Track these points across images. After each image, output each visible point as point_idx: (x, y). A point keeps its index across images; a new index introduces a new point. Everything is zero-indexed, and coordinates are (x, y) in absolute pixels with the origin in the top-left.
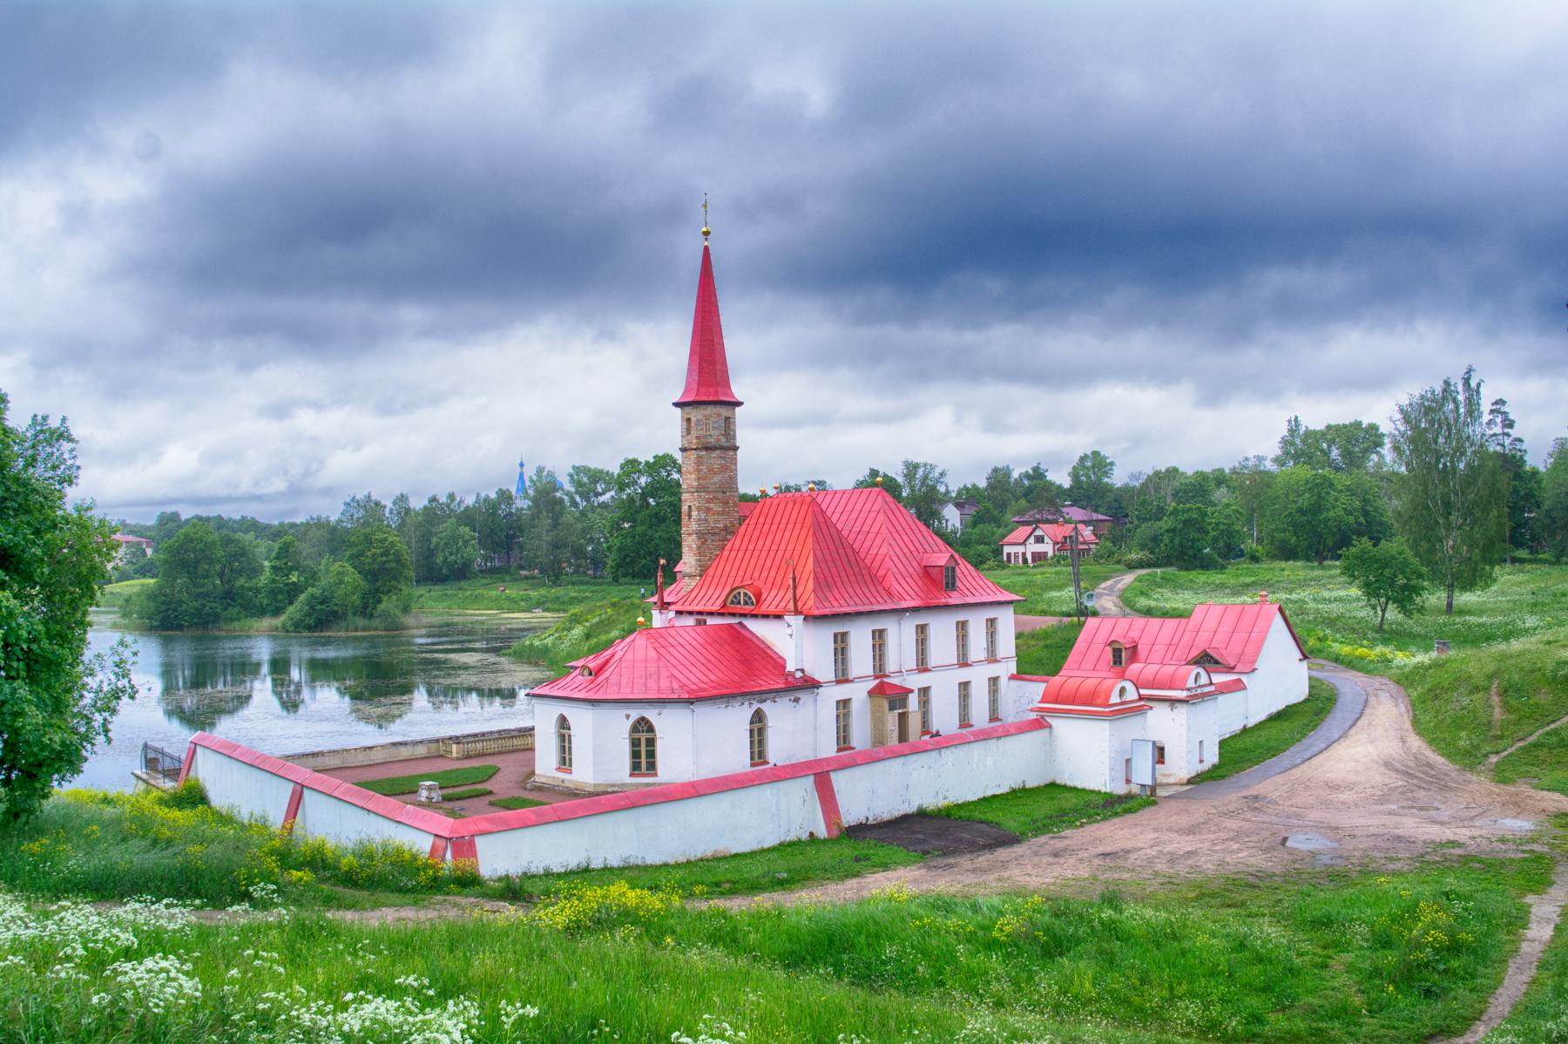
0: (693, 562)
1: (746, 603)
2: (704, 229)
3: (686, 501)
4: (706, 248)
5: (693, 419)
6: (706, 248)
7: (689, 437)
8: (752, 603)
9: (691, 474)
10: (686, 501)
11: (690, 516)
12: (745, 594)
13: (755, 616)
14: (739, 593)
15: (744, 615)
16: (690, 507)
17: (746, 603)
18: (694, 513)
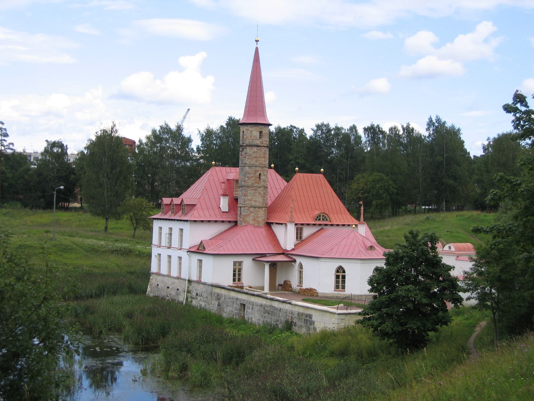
0: (262, 201)
1: (323, 220)
2: (257, 39)
3: (258, 171)
4: (257, 49)
5: (264, 132)
6: (257, 49)
7: (261, 140)
8: (327, 220)
9: (261, 158)
10: (258, 171)
11: (259, 178)
12: (323, 216)
13: (332, 225)
14: (320, 216)
15: (326, 225)
16: (260, 174)
17: (323, 220)
18: (262, 177)
